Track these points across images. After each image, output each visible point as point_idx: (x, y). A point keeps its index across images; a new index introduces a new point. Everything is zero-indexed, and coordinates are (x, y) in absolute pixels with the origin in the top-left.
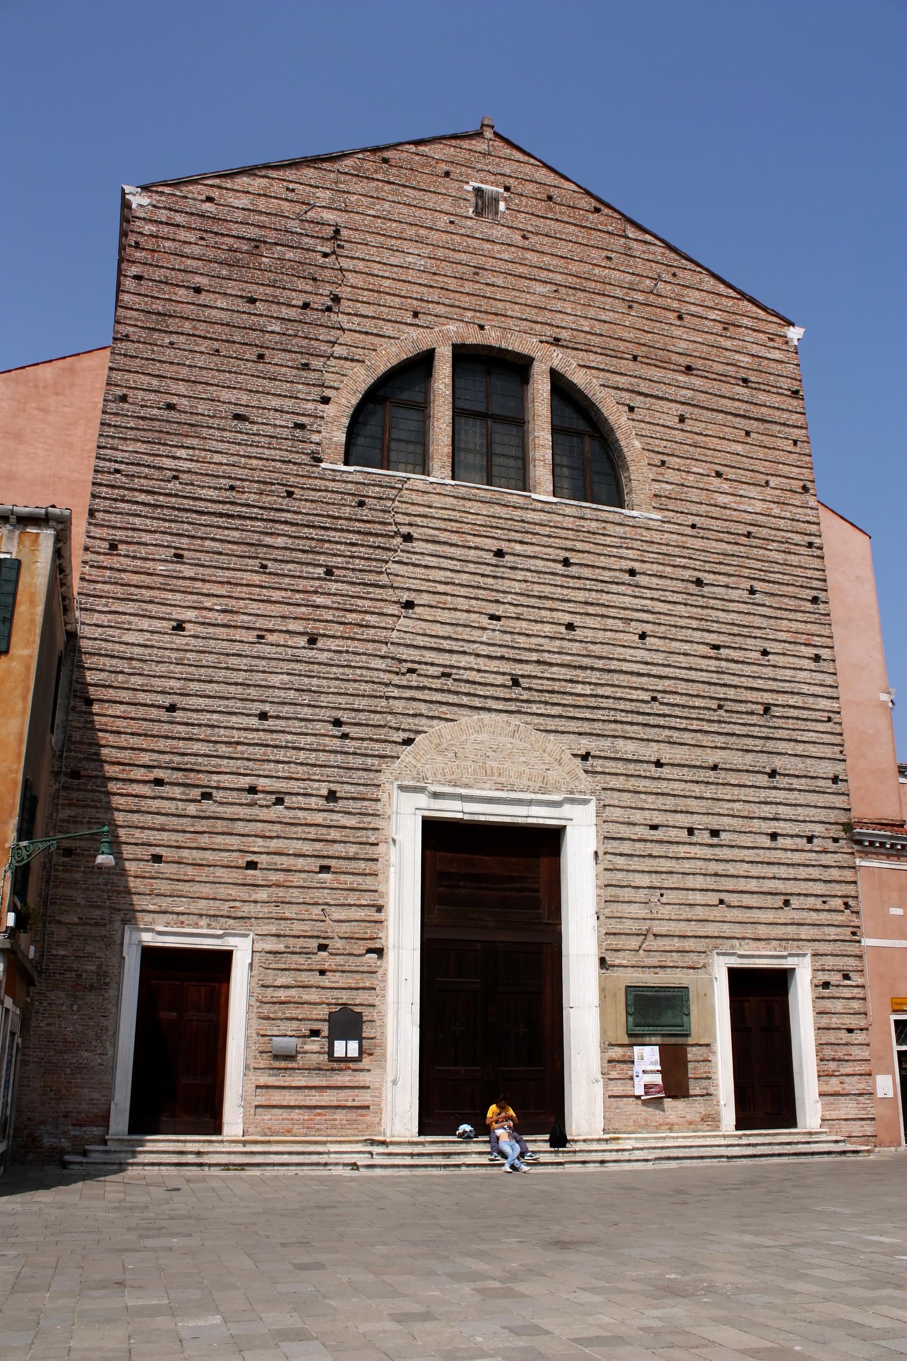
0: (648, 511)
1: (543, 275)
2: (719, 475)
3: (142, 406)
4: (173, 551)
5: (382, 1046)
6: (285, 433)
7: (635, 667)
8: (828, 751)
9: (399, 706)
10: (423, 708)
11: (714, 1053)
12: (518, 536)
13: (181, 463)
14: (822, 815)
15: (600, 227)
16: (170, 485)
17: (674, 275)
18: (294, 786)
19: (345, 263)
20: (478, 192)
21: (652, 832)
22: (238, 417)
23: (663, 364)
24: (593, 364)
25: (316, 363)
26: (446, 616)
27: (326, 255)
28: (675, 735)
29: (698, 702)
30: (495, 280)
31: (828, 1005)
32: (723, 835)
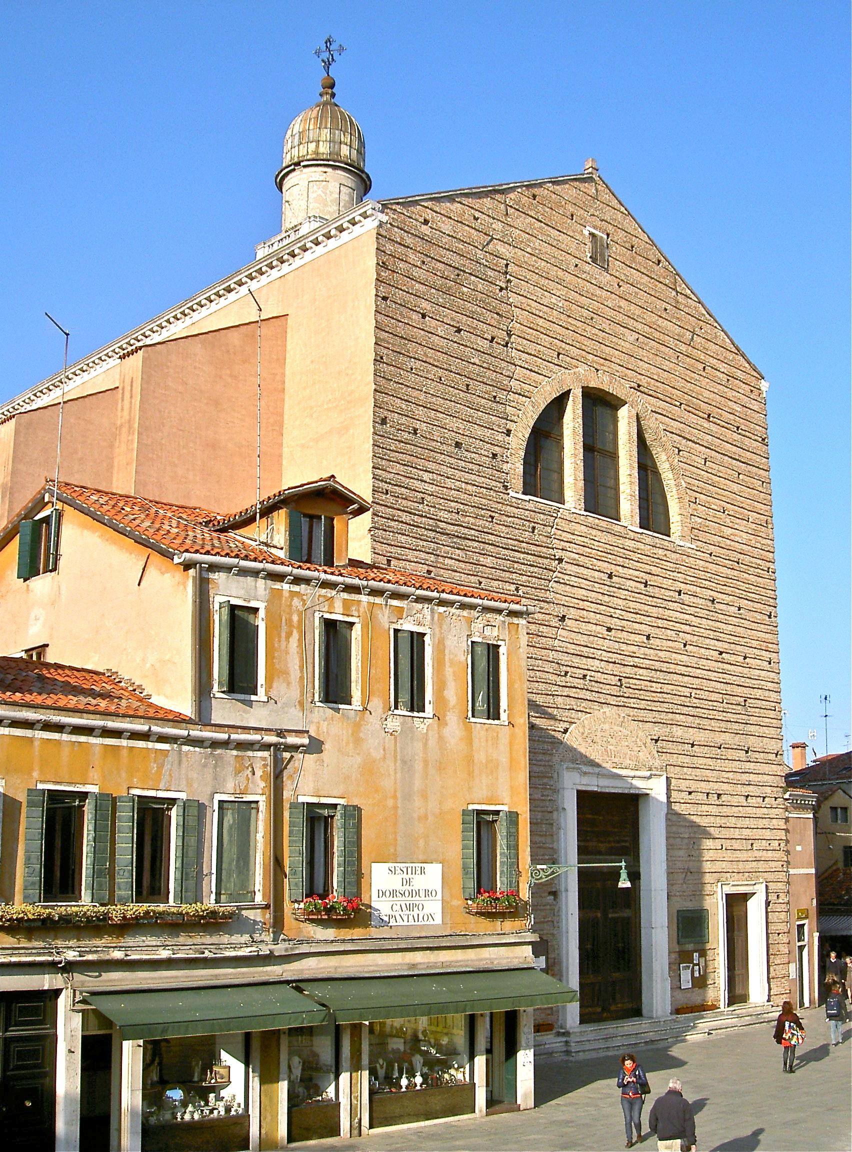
3: (398, 430)
4: (426, 567)
7: (683, 670)
12: (620, 561)
13: (426, 486)
15: (661, 280)
19: (513, 299)
22: (458, 445)
23: (693, 410)
27: (501, 289)
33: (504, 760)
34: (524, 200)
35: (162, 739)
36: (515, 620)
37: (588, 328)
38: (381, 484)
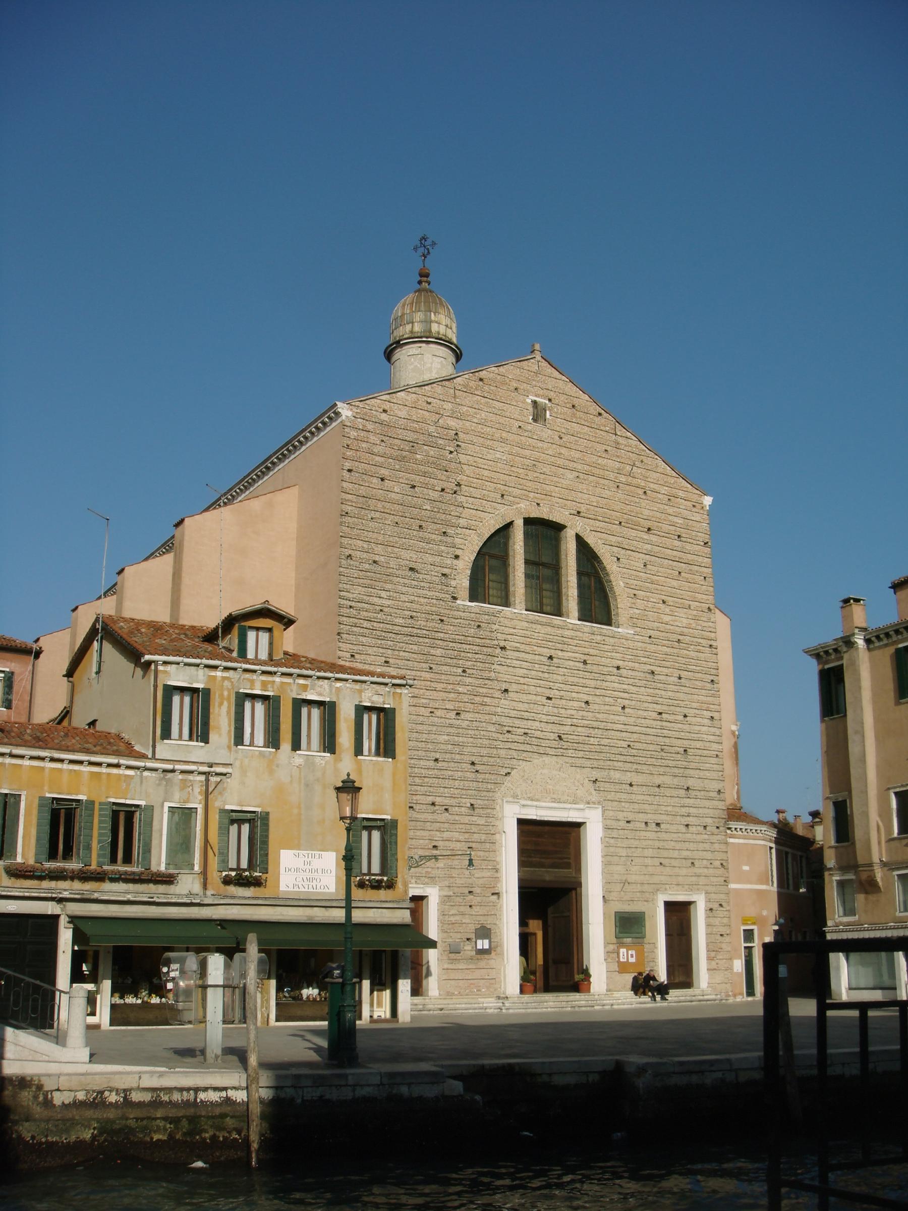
0: (627, 628)
1: (571, 465)
2: (664, 602)
5: (501, 946)
6: (437, 580)
8: (714, 775)
9: (502, 753)
10: (515, 754)
11: (656, 948)
14: (711, 812)
16: (379, 616)
17: (642, 461)
18: (453, 802)
19: (463, 458)
20: (535, 403)
21: (628, 825)
22: (411, 569)
23: (635, 526)
24: (598, 530)
25: (450, 531)
26: (524, 698)
27: (451, 452)
28: (639, 767)
29: (651, 747)
30: (545, 469)
31: (711, 920)
32: (662, 826)
33: (388, 783)
34: (472, 384)
35: (129, 767)
36: (398, 690)
37: (530, 473)
38: (345, 602)
